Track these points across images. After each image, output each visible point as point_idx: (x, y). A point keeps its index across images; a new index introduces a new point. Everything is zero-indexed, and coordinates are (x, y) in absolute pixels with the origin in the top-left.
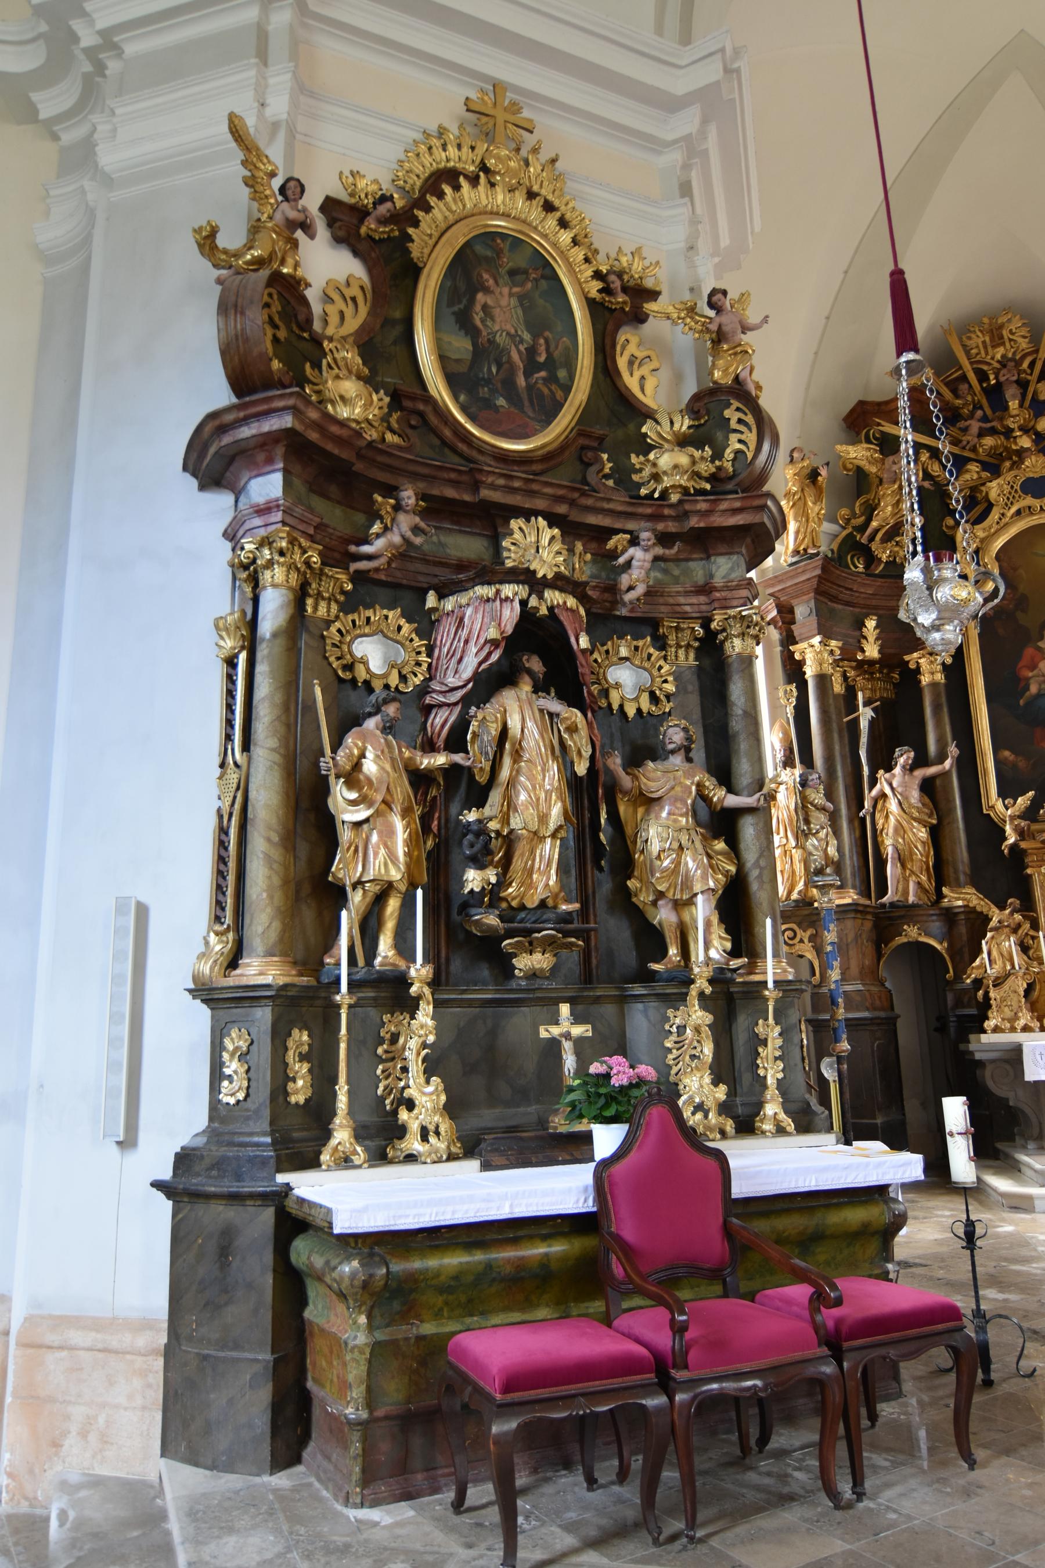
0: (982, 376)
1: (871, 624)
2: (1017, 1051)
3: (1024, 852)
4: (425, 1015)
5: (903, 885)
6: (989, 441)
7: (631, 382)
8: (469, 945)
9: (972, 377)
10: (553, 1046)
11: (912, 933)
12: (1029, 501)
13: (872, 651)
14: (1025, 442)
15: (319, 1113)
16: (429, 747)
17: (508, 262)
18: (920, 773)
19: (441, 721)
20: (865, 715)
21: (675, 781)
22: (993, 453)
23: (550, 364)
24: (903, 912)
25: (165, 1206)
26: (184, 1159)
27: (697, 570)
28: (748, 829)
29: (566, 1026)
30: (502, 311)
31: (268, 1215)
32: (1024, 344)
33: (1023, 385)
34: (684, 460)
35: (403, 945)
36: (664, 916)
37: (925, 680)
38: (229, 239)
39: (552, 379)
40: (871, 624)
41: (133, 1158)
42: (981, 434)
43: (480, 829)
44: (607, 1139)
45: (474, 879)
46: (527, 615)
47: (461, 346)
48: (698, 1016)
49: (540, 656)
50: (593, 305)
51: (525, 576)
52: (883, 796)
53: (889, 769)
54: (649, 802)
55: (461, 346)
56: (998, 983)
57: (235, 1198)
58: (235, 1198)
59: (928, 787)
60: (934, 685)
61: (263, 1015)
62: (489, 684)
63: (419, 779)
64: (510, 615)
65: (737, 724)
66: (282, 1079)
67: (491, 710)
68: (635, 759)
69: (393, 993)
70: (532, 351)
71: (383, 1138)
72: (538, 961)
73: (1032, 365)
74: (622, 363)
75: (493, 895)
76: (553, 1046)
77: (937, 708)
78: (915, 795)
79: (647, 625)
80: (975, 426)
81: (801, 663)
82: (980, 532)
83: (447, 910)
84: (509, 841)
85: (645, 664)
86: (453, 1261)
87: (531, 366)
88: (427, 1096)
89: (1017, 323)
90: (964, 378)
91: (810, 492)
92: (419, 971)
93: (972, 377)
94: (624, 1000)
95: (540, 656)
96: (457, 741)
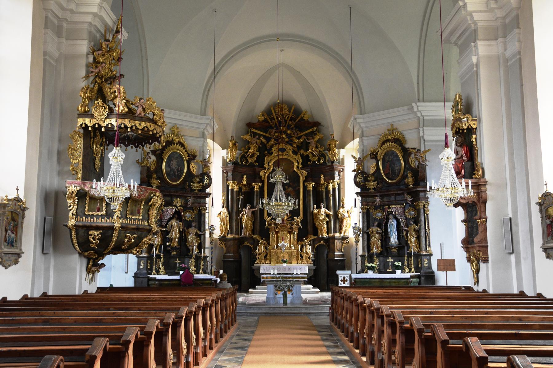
0: (277, 118)
1: (245, 177)
2: (260, 267)
3: (269, 229)
4: (162, 259)
5: (245, 233)
6: (277, 134)
7: (192, 170)
8: (167, 252)
9: (275, 118)
10: (176, 263)
11: (246, 243)
12: (280, 153)
13: (245, 182)
14: (284, 136)
15: (151, 270)
16: (163, 227)
17: (175, 156)
18: (251, 210)
19: (164, 223)
20: (241, 197)
21: (193, 231)
22: (277, 137)
23: (181, 171)
24: (245, 239)
25: (133, 279)
26: (135, 274)
27: (199, 200)
28: (202, 237)
29: (178, 261)
30: (174, 163)
31: (147, 279)
32: (287, 112)
33: (286, 121)
34: (198, 185)
35: (160, 251)
36: (190, 248)
37: (255, 190)
38: (140, 161)
39: (181, 173)
40: (245, 177)
41: (127, 274)
42: (275, 132)
43: (169, 238)
44: (181, 272)
45: (168, 244)
46: (176, 211)
47: (168, 169)
48: (193, 260)
49: (177, 215)
50: (187, 160)
51: (175, 206)
52: (243, 214)
53: (246, 208)
54: (190, 234)
55: (168, 169)
56: (259, 254)
57: (143, 277)
58: (143, 277)
59: (253, 213)
60: (257, 191)
61: (146, 259)
62: (170, 219)
63: (161, 231)
64: (174, 211)
65: (202, 223)
66: (147, 266)
67: (170, 223)
68: (188, 228)
69: (158, 257)
70: (178, 169)
71: (158, 272)
72: (175, 253)
73: (288, 118)
74: (191, 167)
75: (170, 246)
76: (176, 263)
77: (257, 196)
78: (250, 214)
79: (192, 208)
80: (274, 131)
81: (229, 185)
82: (270, 158)
83: (165, 247)
84: (172, 239)
85: (190, 213)
86: (167, 282)
87: (178, 171)
88: (162, 268)
89: (286, 107)
90: (274, 117)
91: (234, 147)
92: (162, 254)
93: (275, 118)
94: (184, 258)
95: (177, 215)
96: (166, 227)
